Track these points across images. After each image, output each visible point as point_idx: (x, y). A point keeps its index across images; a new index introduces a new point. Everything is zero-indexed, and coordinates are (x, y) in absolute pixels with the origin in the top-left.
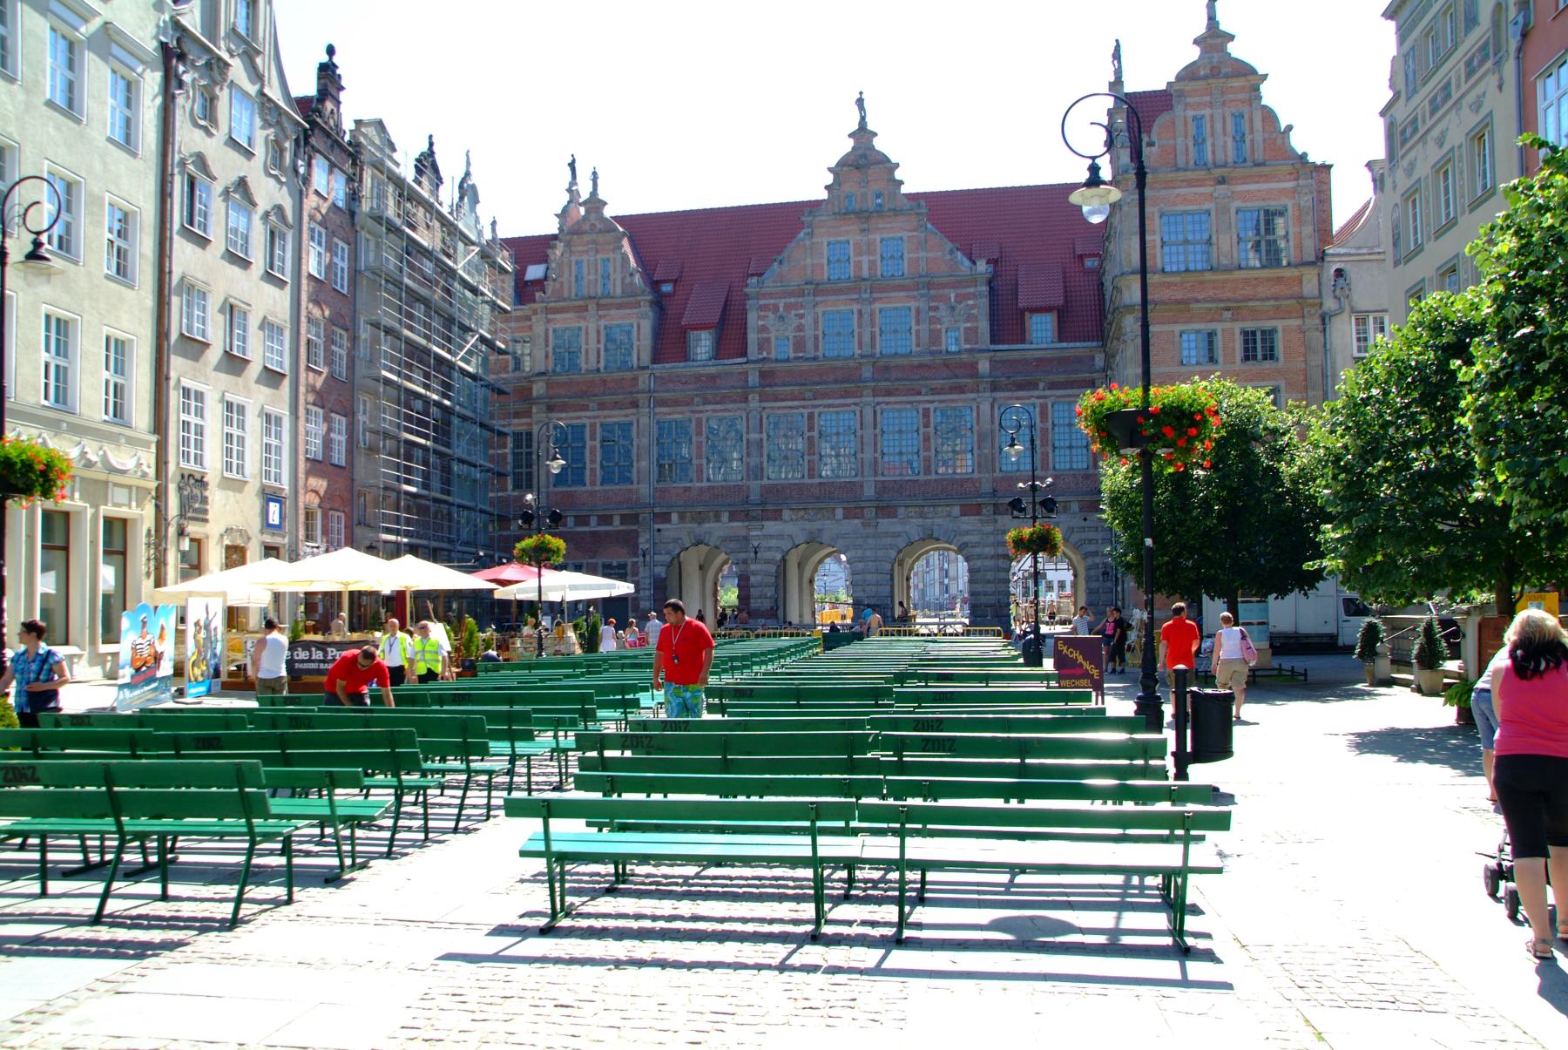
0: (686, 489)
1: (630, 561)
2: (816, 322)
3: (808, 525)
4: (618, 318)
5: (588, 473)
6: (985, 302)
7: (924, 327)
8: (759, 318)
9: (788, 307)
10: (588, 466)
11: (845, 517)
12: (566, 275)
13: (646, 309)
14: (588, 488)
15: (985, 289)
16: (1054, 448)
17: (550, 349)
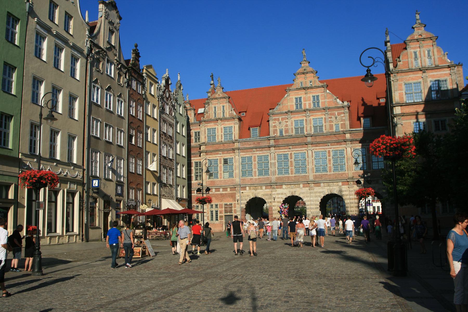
0: (251, 179)
1: (233, 203)
2: (292, 123)
3: (291, 190)
4: (228, 124)
5: (219, 174)
6: (348, 114)
7: (328, 124)
8: (274, 123)
9: (282, 119)
10: (219, 172)
11: (304, 187)
12: (211, 111)
13: (237, 121)
14: (219, 179)
15: (347, 110)
16: (373, 162)
17: (206, 135)
